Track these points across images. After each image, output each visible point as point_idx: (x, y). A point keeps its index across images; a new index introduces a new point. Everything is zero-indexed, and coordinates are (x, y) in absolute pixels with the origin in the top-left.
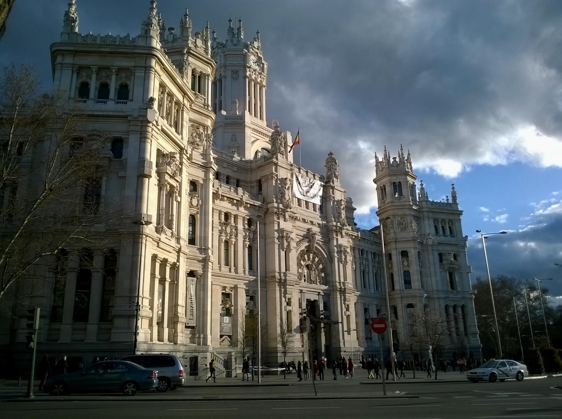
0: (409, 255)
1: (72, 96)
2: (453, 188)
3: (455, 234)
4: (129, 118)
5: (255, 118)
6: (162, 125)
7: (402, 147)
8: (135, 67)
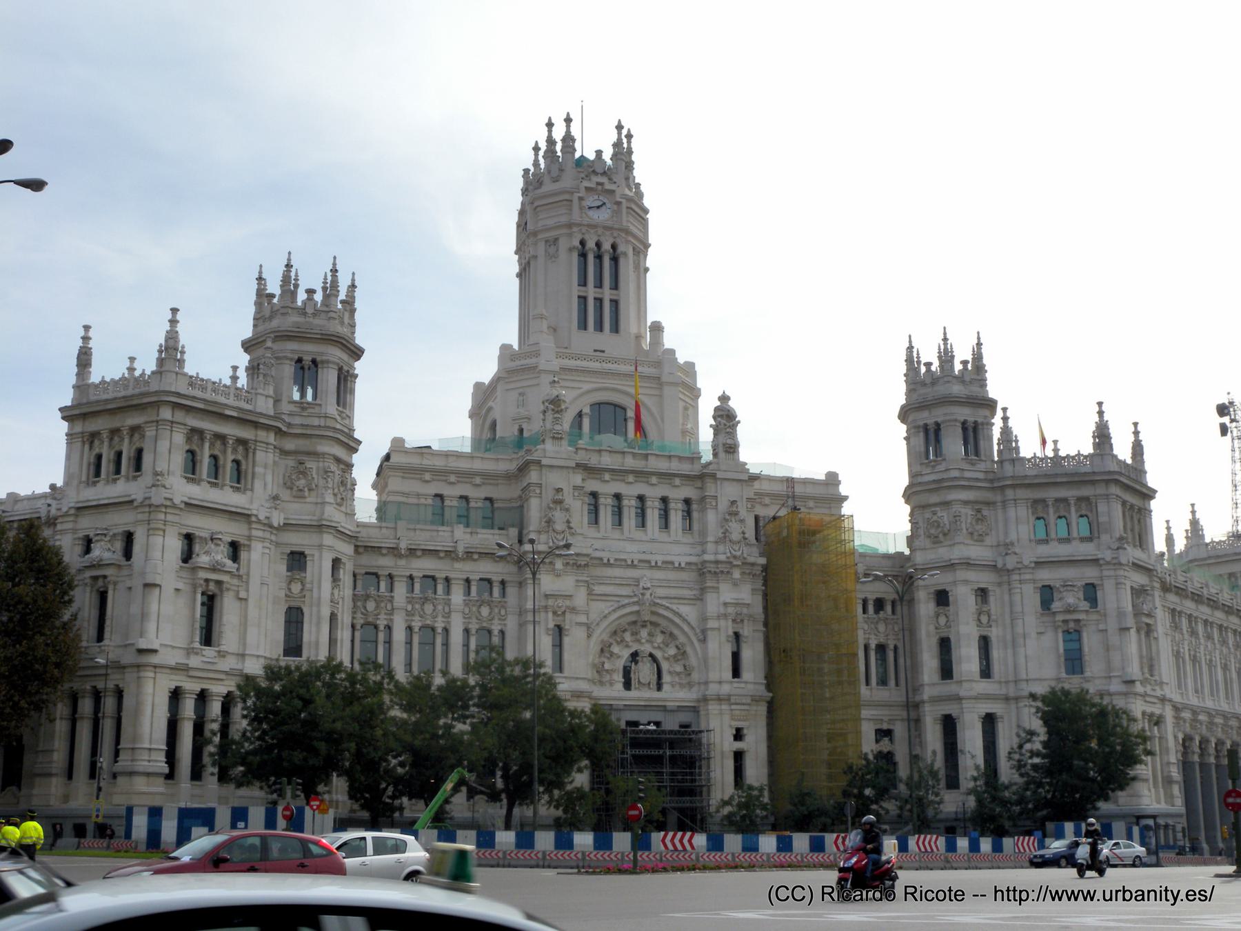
1: (84, 479)
2: (1101, 413)
3: (1096, 535)
4: (135, 504)
5: (598, 334)
6: (186, 499)
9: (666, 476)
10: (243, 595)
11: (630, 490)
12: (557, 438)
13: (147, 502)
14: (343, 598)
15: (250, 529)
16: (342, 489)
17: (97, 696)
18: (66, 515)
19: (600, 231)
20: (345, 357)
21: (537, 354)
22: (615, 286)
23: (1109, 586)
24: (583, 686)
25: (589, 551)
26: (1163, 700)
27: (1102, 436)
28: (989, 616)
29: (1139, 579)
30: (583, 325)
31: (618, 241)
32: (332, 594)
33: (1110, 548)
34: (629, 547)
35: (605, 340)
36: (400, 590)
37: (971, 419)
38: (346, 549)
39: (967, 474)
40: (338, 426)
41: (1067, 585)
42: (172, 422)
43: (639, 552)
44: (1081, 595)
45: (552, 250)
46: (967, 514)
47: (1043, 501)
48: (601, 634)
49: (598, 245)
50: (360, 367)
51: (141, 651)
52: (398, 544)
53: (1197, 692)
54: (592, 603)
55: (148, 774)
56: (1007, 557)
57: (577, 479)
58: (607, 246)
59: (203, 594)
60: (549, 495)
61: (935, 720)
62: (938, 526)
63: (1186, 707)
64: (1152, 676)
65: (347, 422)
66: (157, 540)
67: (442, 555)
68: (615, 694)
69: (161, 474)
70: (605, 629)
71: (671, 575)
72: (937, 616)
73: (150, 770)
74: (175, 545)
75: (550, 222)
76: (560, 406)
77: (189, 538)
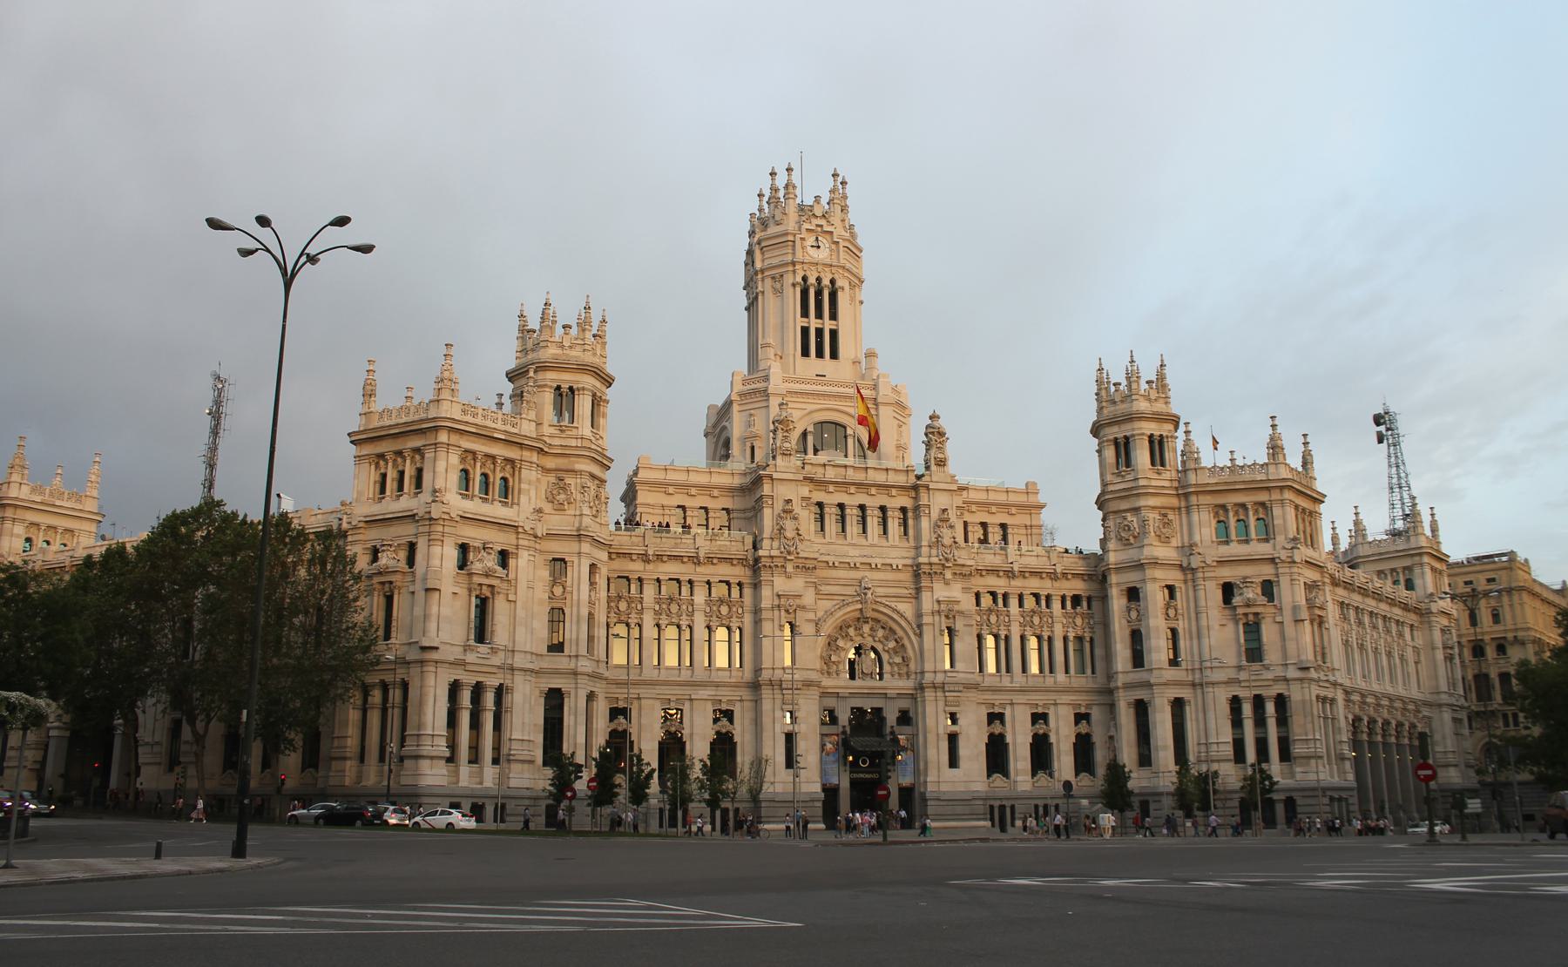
0: (1141, 595)
1: (371, 496)
3: (1272, 536)
4: (417, 518)
6: (461, 513)
7: (1132, 356)
8: (424, 446)
9: (885, 487)
10: (511, 597)
11: (872, 502)
12: (786, 455)
13: (427, 516)
14: (599, 600)
15: (517, 538)
16: (597, 502)
17: (385, 687)
18: (355, 528)
19: (820, 268)
20: (598, 384)
21: (766, 379)
22: (833, 316)
23: (1284, 582)
24: (814, 676)
25: (816, 556)
26: (1335, 684)
27: (1275, 448)
28: (1176, 610)
29: (1312, 575)
30: (805, 352)
31: (836, 276)
32: (590, 596)
33: (1285, 548)
34: (853, 552)
35: (826, 365)
36: (649, 592)
37: (1157, 433)
38: (604, 556)
39: (1154, 483)
40: (593, 447)
41: (1245, 580)
42: (448, 445)
43: (860, 556)
44: (1259, 591)
45: (778, 285)
46: (1154, 518)
47: (1223, 507)
48: (828, 628)
49: (819, 280)
50: (610, 393)
51: (424, 649)
52: (646, 551)
53: (1364, 677)
54: (819, 602)
55: (432, 758)
56: (1191, 557)
57: (805, 491)
58: (826, 282)
59: (477, 597)
60: (779, 506)
61: (1129, 704)
62: (1129, 529)
63: (1355, 690)
64: (1324, 663)
65: (600, 442)
66: (436, 550)
67: (685, 560)
68: (842, 683)
69: (439, 491)
70: (832, 624)
71: (890, 576)
72: (1129, 610)
73: (434, 754)
74: (452, 554)
75: (775, 261)
76: (788, 426)
77: (464, 548)
